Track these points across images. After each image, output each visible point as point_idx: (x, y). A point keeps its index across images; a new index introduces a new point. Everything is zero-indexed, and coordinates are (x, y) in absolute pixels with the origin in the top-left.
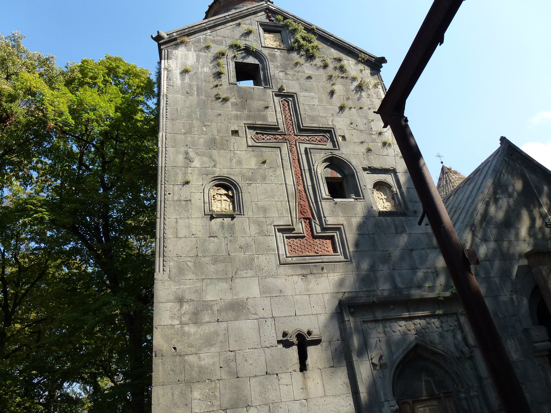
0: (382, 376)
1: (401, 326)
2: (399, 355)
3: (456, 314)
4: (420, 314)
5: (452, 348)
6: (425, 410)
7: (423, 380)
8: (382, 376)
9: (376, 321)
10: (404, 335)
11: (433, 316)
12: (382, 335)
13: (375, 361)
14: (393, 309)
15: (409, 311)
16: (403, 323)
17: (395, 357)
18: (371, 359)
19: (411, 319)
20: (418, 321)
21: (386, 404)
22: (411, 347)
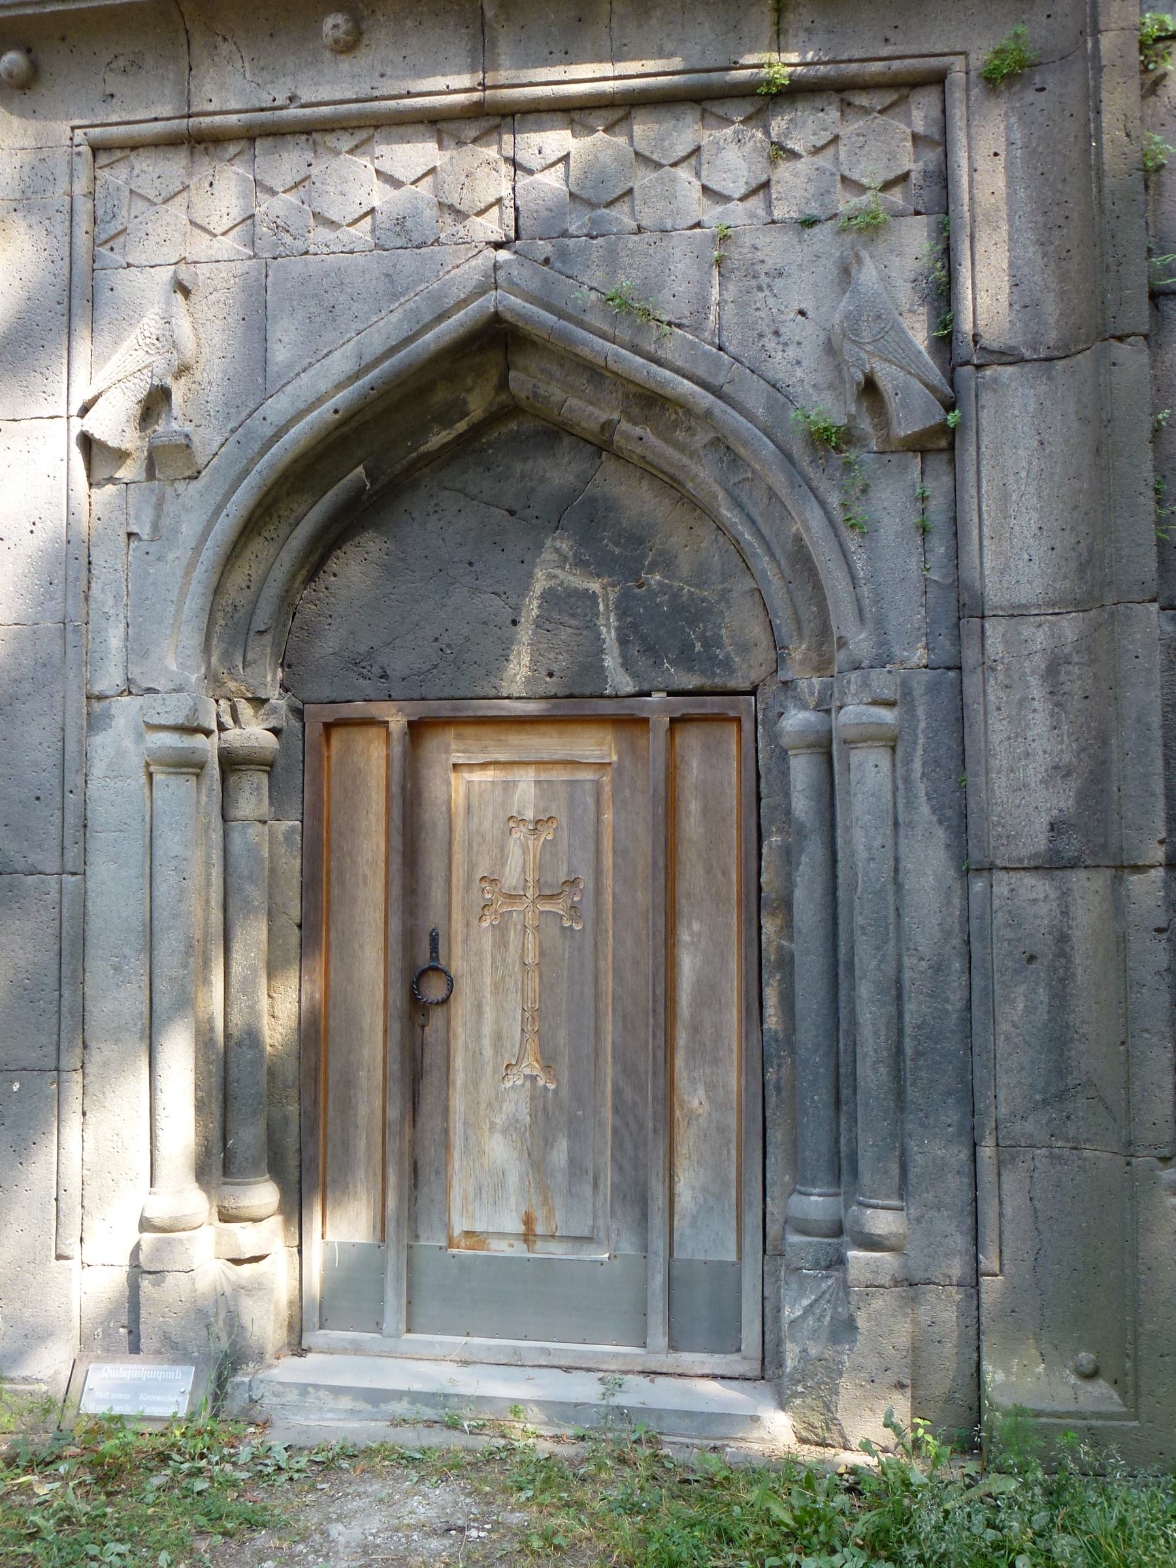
0: (145, 532)
1: (396, 183)
2: (319, 381)
3: (938, 79)
4: (586, 77)
5: (797, 362)
6: (508, 786)
7: (540, 584)
8: (145, 532)
9: (201, 142)
10: (402, 235)
11: (701, 99)
12: (229, 246)
13: (113, 423)
14: (348, 46)
15: (481, 56)
16: (414, 155)
17: (278, 407)
18: (85, 410)
19: (493, 118)
20: (556, 140)
21: (126, 710)
22: (431, 340)
